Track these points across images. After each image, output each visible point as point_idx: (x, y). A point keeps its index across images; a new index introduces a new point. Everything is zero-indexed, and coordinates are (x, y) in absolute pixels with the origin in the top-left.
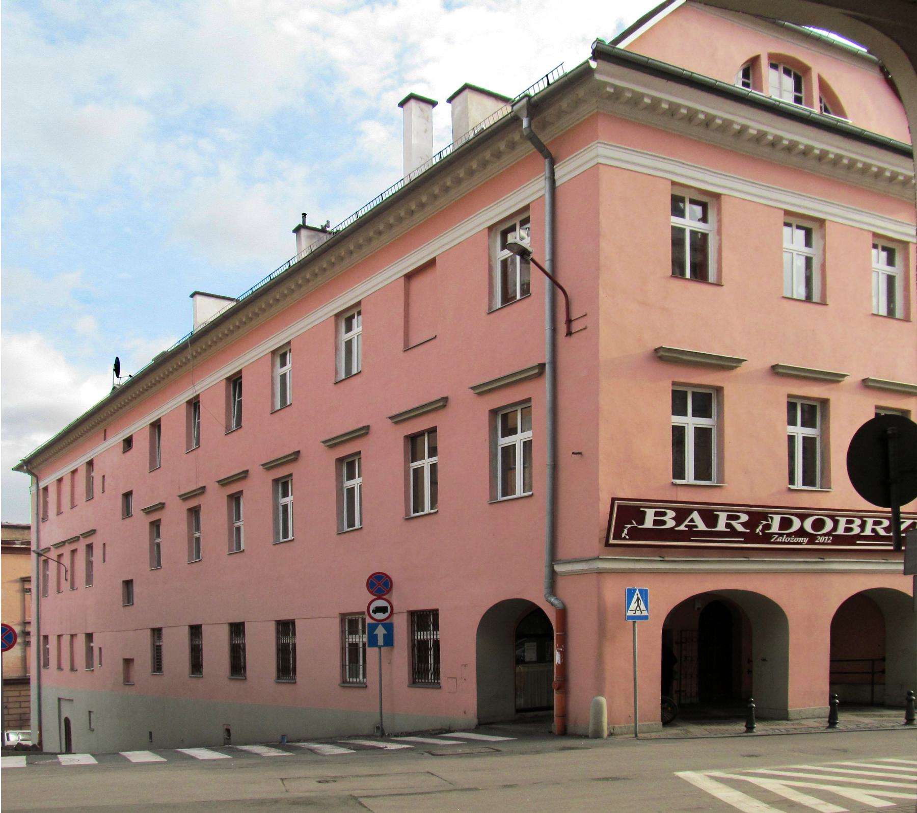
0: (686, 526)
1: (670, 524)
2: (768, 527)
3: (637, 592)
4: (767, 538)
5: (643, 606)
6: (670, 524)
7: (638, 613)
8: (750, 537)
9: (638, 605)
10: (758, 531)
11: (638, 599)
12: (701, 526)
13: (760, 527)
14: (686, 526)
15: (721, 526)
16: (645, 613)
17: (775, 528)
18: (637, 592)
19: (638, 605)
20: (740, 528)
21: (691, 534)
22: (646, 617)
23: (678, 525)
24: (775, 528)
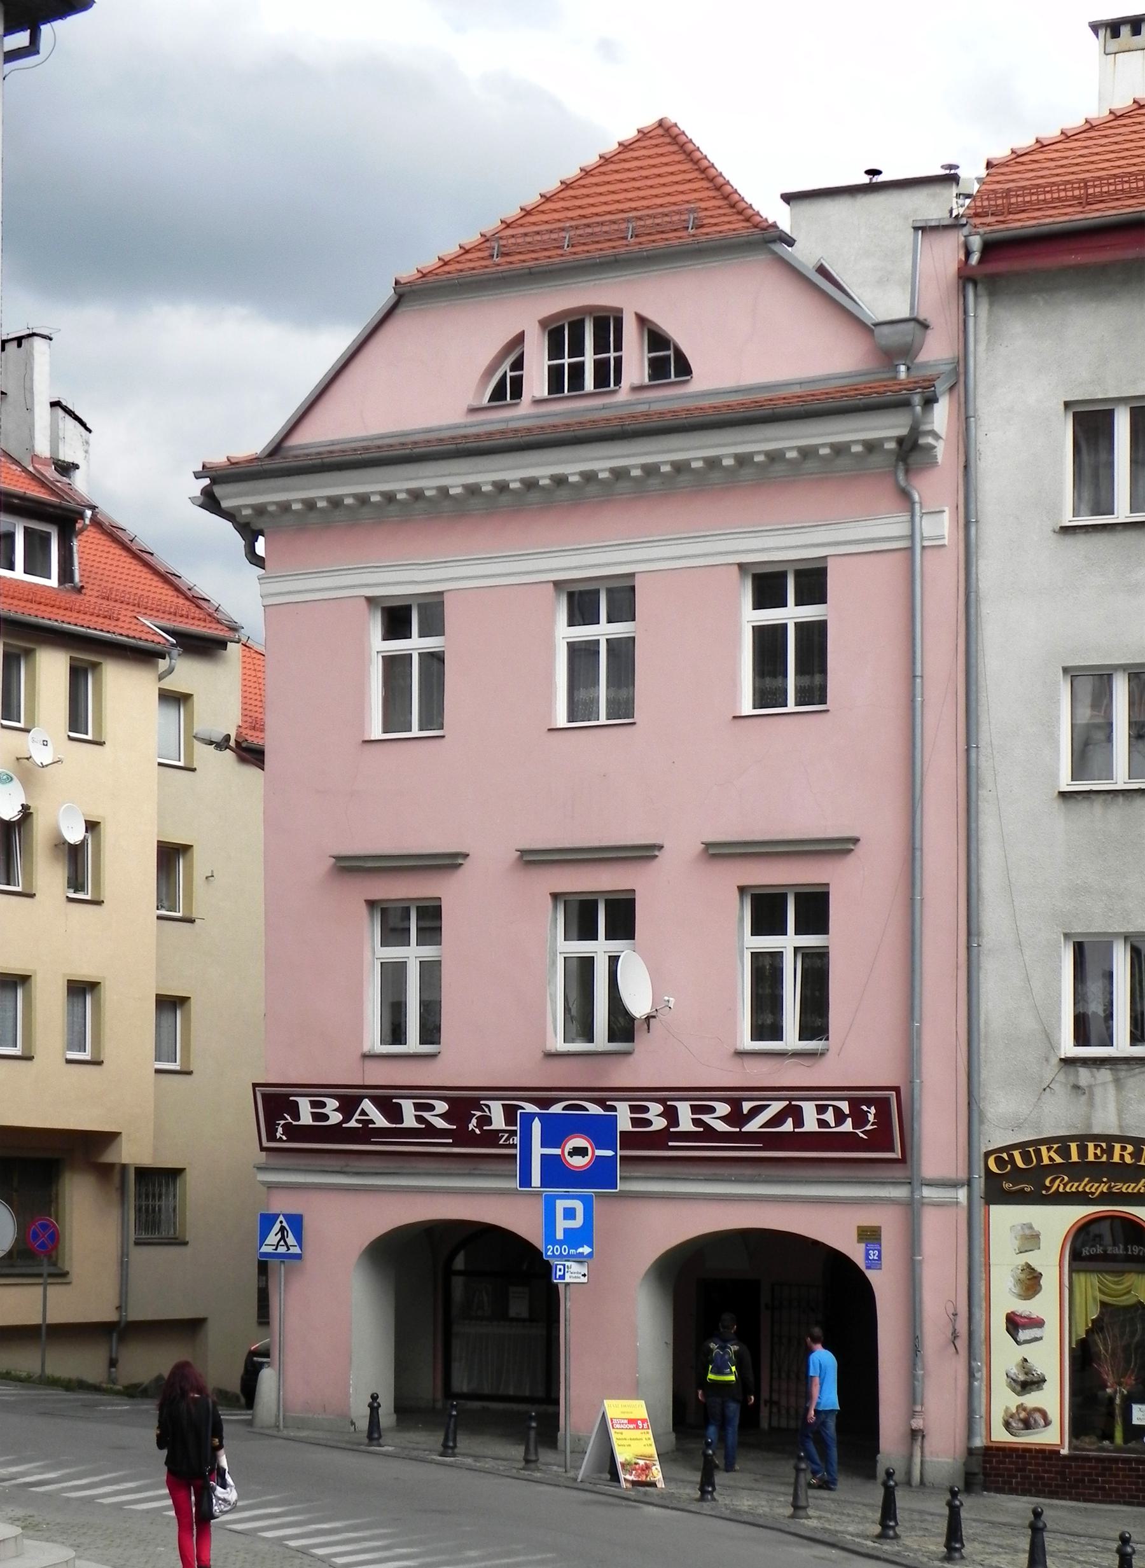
0: (358, 1121)
1: (335, 1118)
2: (487, 1120)
3: (281, 1218)
4: (492, 1138)
5: (291, 1240)
6: (335, 1118)
7: (282, 1250)
8: (462, 1137)
9: (283, 1238)
10: (471, 1127)
11: (282, 1229)
12: (381, 1121)
13: (474, 1121)
14: (358, 1121)
15: (409, 1120)
16: (296, 1250)
17: (498, 1122)
18: (281, 1218)
19: (283, 1238)
20: (440, 1124)
21: (367, 1132)
22: (298, 1257)
23: (347, 1119)
24: (498, 1122)
